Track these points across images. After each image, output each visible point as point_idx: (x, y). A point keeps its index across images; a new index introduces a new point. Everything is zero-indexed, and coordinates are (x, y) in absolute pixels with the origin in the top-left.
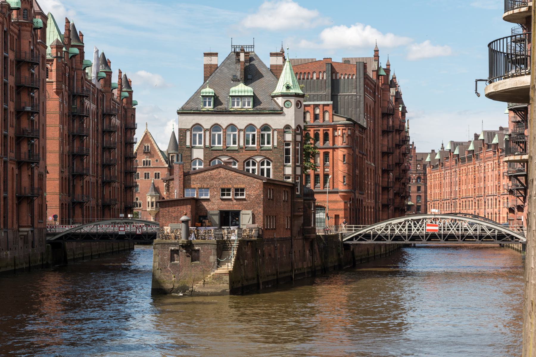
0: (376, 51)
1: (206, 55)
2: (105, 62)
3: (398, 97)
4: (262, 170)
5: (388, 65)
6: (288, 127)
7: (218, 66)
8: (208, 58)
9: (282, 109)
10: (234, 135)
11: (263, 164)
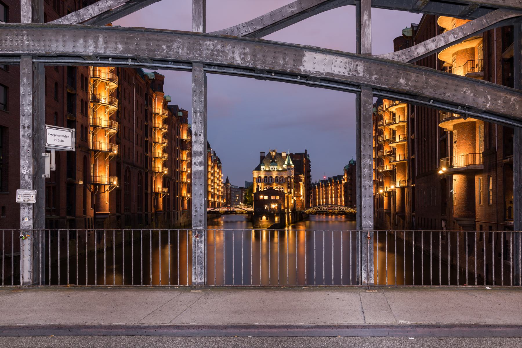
0: (306, 150)
1: (261, 153)
2: (215, 154)
3: (310, 165)
4: (281, 190)
5: (308, 155)
6: (289, 176)
7: (265, 156)
8: (262, 154)
9: (287, 170)
10: (272, 179)
11: (281, 188)
